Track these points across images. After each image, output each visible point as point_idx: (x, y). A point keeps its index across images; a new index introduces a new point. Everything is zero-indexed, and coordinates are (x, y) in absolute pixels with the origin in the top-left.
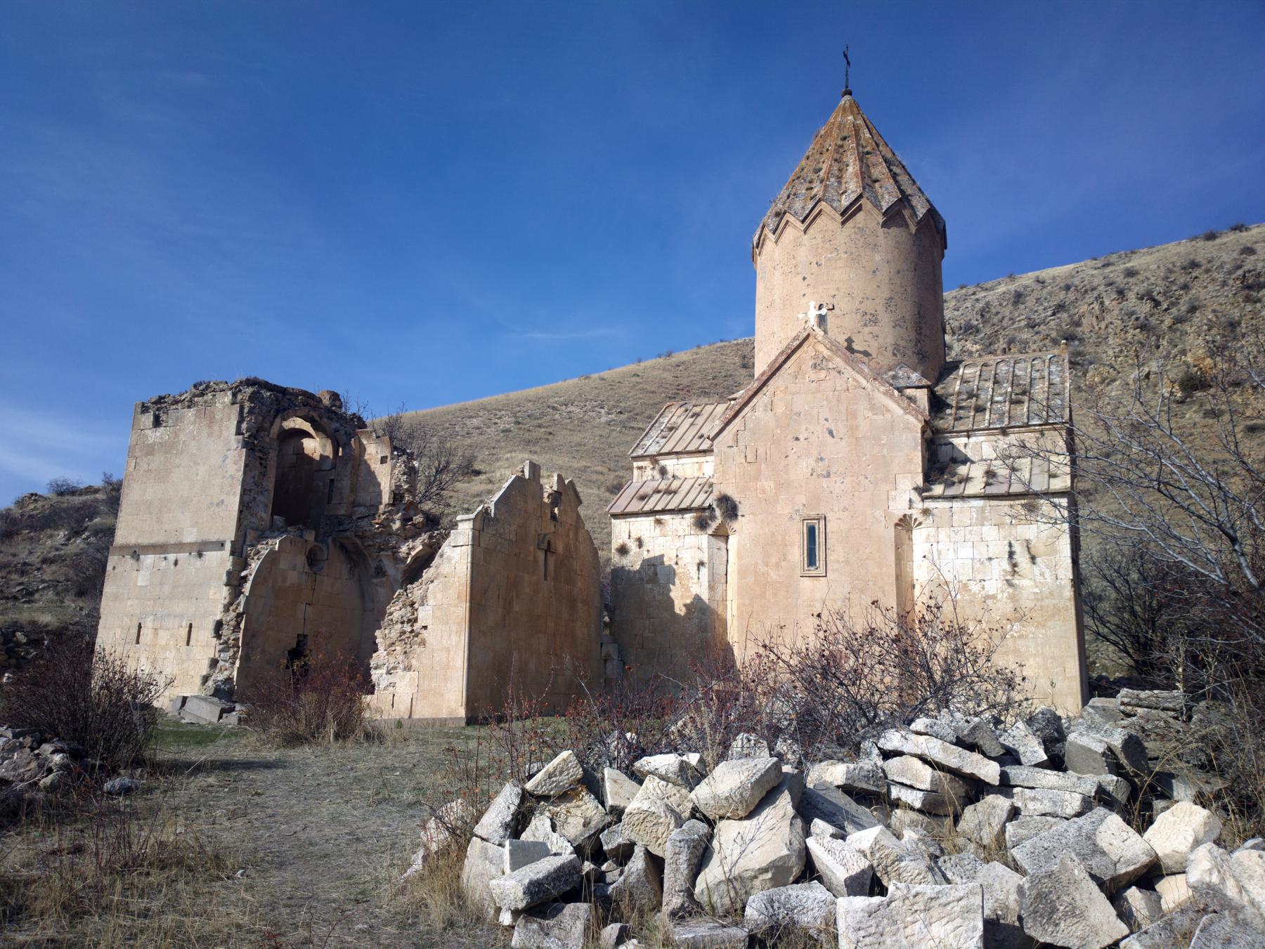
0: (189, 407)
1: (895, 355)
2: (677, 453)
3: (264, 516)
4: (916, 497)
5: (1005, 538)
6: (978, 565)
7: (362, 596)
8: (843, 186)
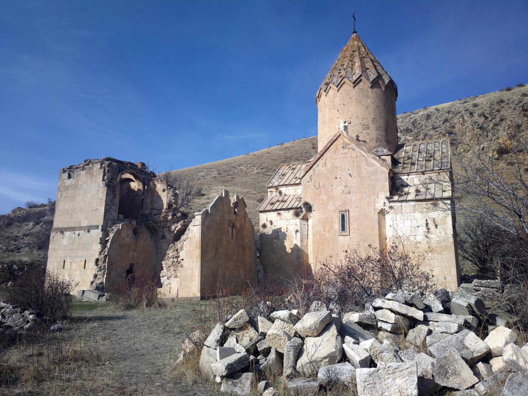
0: (83, 170)
1: (377, 142)
2: (286, 185)
3: (115, 214)
4: (386, 201)
5: (424, 218)
6: (413, 229)
7: (156, 246)
8: (354, 71)
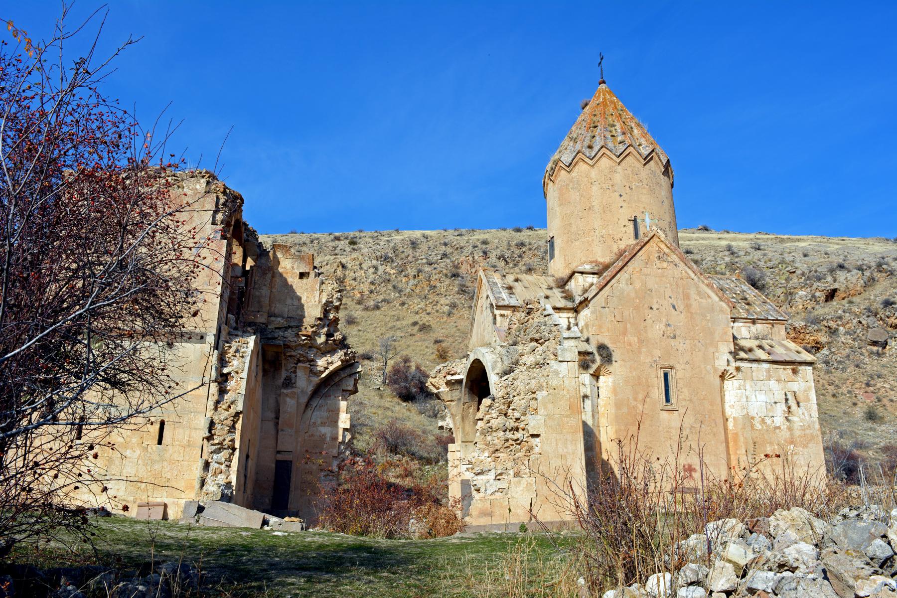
6: (769, 407)
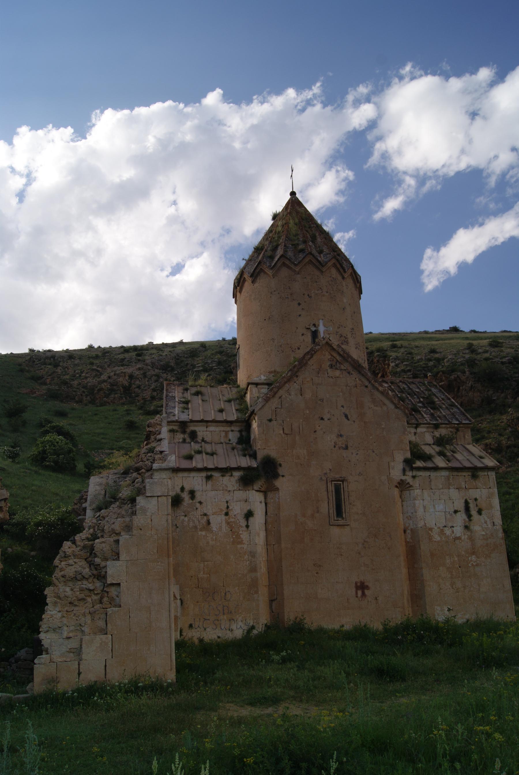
2: (207, 422)
6: (448, 516)
